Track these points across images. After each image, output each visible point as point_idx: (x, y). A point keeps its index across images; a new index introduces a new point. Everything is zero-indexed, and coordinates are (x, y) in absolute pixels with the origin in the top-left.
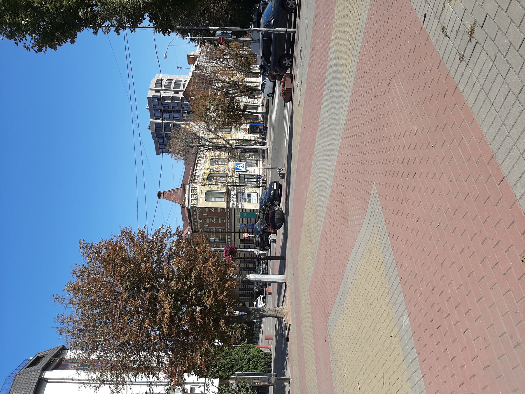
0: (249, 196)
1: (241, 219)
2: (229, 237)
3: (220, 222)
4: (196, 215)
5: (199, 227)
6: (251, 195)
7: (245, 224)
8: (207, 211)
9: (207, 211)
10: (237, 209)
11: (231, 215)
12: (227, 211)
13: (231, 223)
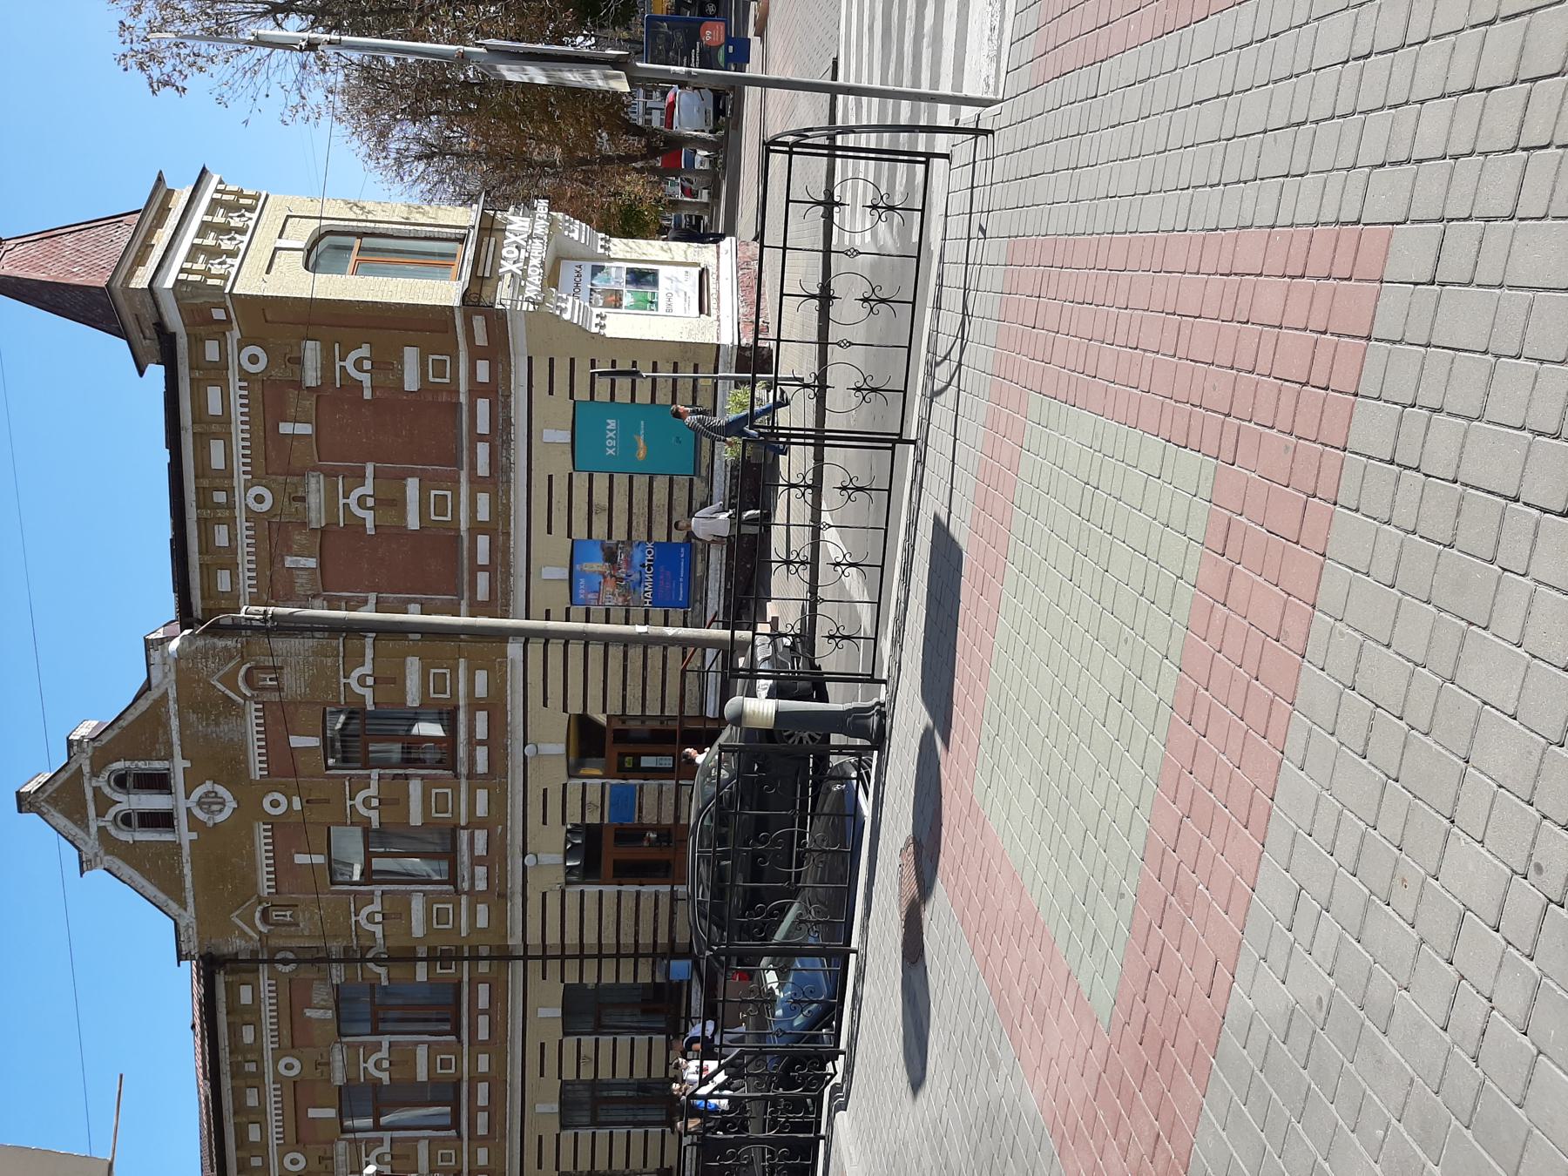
0: (642, 277)
1: (581, 480)
2: (481, 677)
3: (413, 522)
4: (225, 419)
5: (246, 584)
6: (655, 273)
7: (610, 556)
8: (311, 378)
9: (311, 378)
10: (544, 319)
11: (500, 434)
12: (477, 390)
13: (497, 530)
